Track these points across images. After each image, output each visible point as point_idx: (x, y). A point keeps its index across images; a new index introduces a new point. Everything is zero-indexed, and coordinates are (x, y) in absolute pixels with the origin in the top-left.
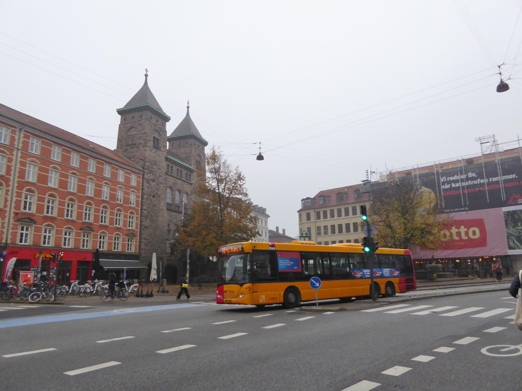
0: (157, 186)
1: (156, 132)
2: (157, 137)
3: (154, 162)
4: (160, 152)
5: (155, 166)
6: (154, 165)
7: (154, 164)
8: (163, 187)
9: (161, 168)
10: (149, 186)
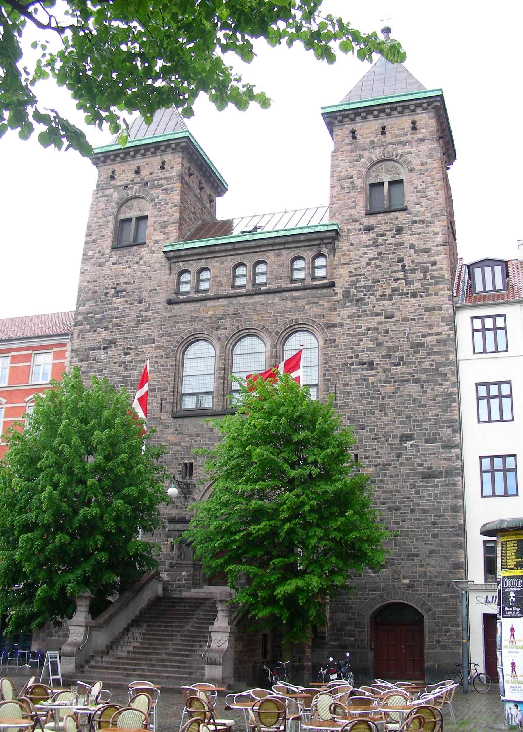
0: (126, 354)
1: (135, 203)
2: (139, 214)
3: (113, 291)
4: (144, 251)
5: (119, 300)
6: (114, 299)
7: (113, 296)
8: (159, 347)
9: (144, 294)
10: (92, 368)
